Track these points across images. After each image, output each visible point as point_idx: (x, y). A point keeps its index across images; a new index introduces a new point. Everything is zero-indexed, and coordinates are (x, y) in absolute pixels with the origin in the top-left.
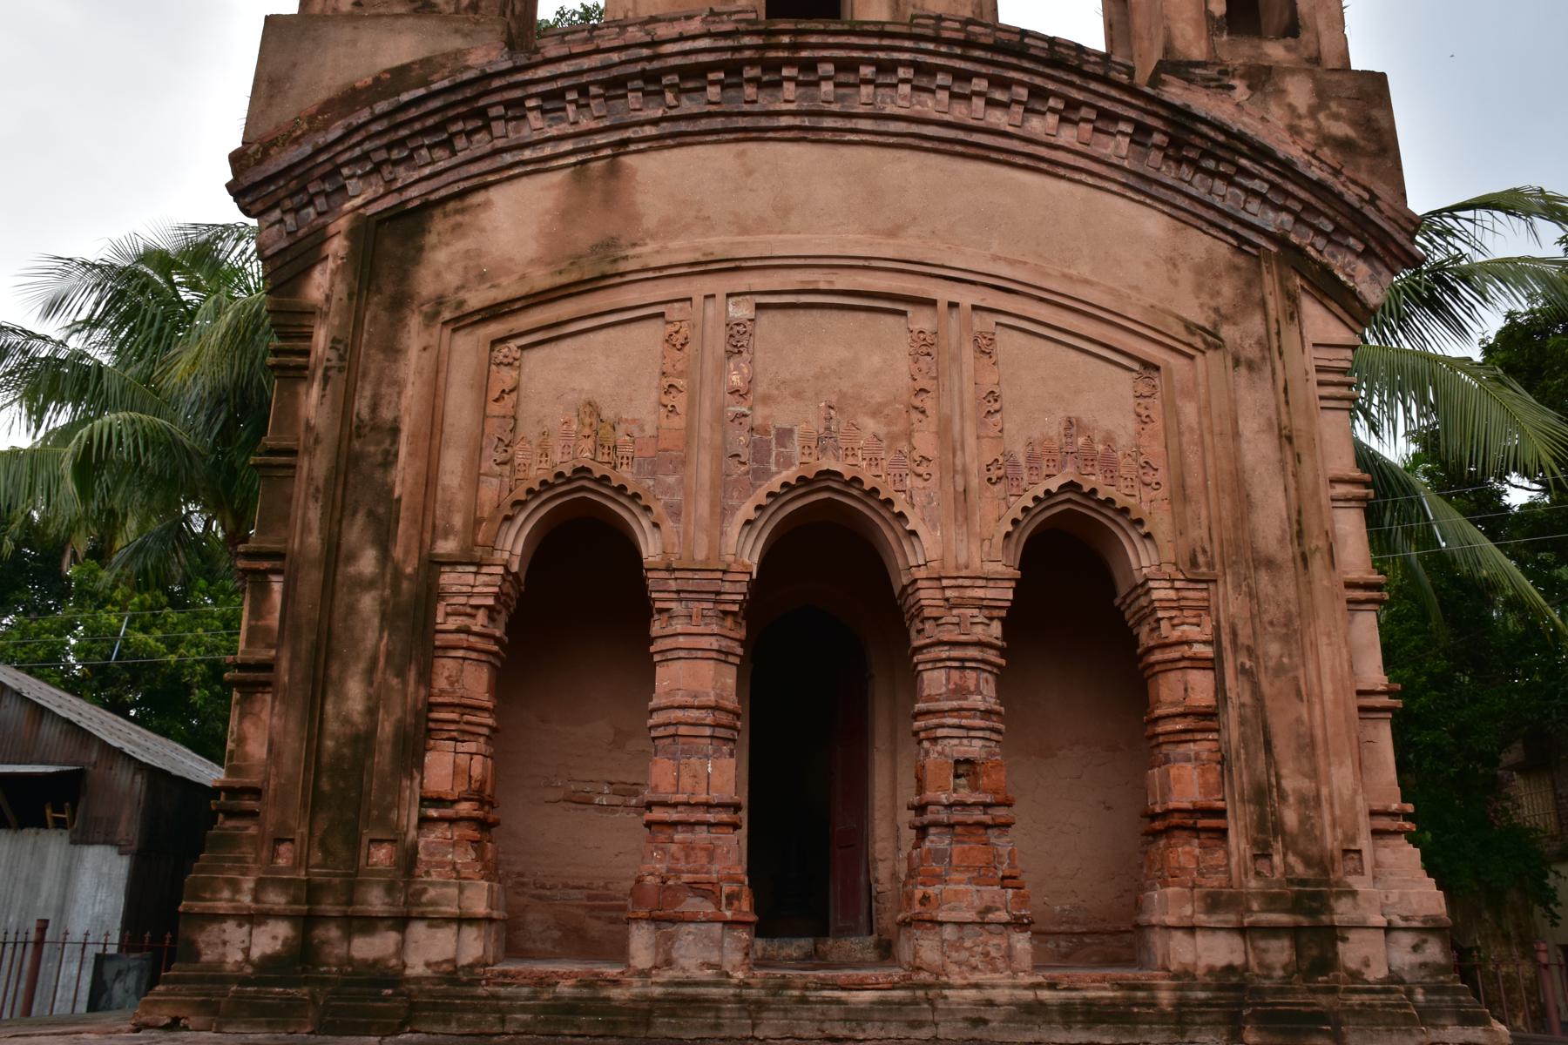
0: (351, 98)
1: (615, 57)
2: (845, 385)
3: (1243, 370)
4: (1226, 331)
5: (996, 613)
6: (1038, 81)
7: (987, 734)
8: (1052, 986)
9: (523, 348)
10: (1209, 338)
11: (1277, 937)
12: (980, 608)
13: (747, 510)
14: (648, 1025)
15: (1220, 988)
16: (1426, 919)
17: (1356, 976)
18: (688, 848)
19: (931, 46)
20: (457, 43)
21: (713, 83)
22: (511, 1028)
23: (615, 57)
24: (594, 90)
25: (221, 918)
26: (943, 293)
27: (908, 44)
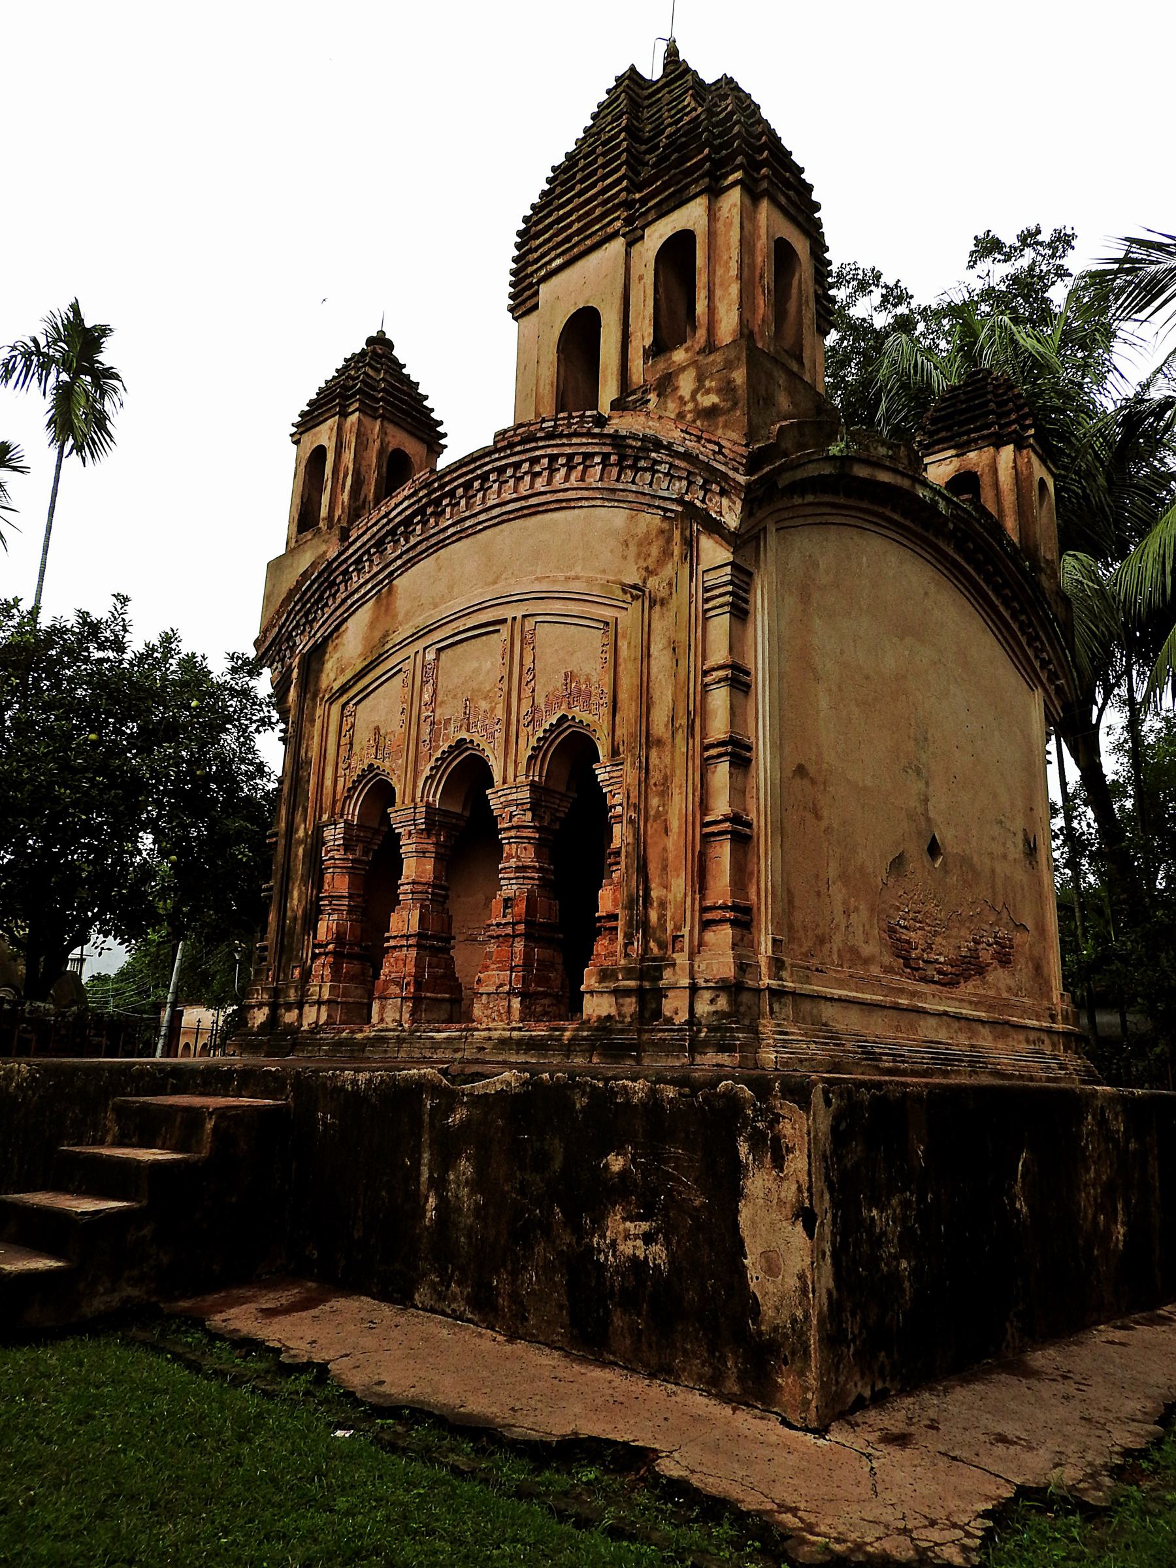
0: (291, 593)
1: (375, 529)
2: (475, 685)
3: (658, 607)
4: (652, 582)
5: (525, 807)
6: (549, 451)
7: (521, 881)
8: (520, 1029)
9: (356, 704)
10: (635, 592)
11: (629, 997)
12: (517, 805)
13: (427, 772)
14: (363, 1051)
15: (597, 1029)
16: (723, 980)
17: (669, 1020)
18: (397, 959)
19: (497, 456)
20: (324, 548)
21: (417, 523)
22: (322, 1053)
23: (375, 529)
24: (373, 550)
25: (253, 1007)
26: (508, 612)
27: (487, 459)
